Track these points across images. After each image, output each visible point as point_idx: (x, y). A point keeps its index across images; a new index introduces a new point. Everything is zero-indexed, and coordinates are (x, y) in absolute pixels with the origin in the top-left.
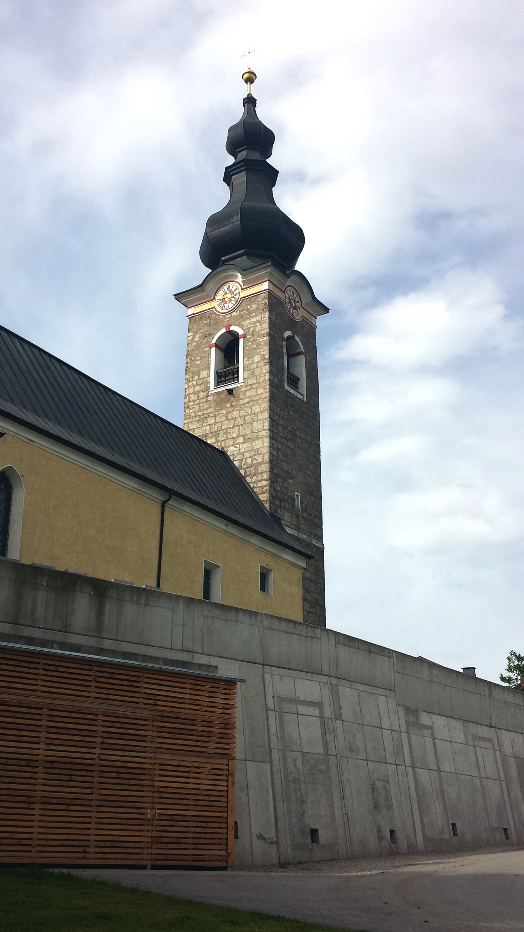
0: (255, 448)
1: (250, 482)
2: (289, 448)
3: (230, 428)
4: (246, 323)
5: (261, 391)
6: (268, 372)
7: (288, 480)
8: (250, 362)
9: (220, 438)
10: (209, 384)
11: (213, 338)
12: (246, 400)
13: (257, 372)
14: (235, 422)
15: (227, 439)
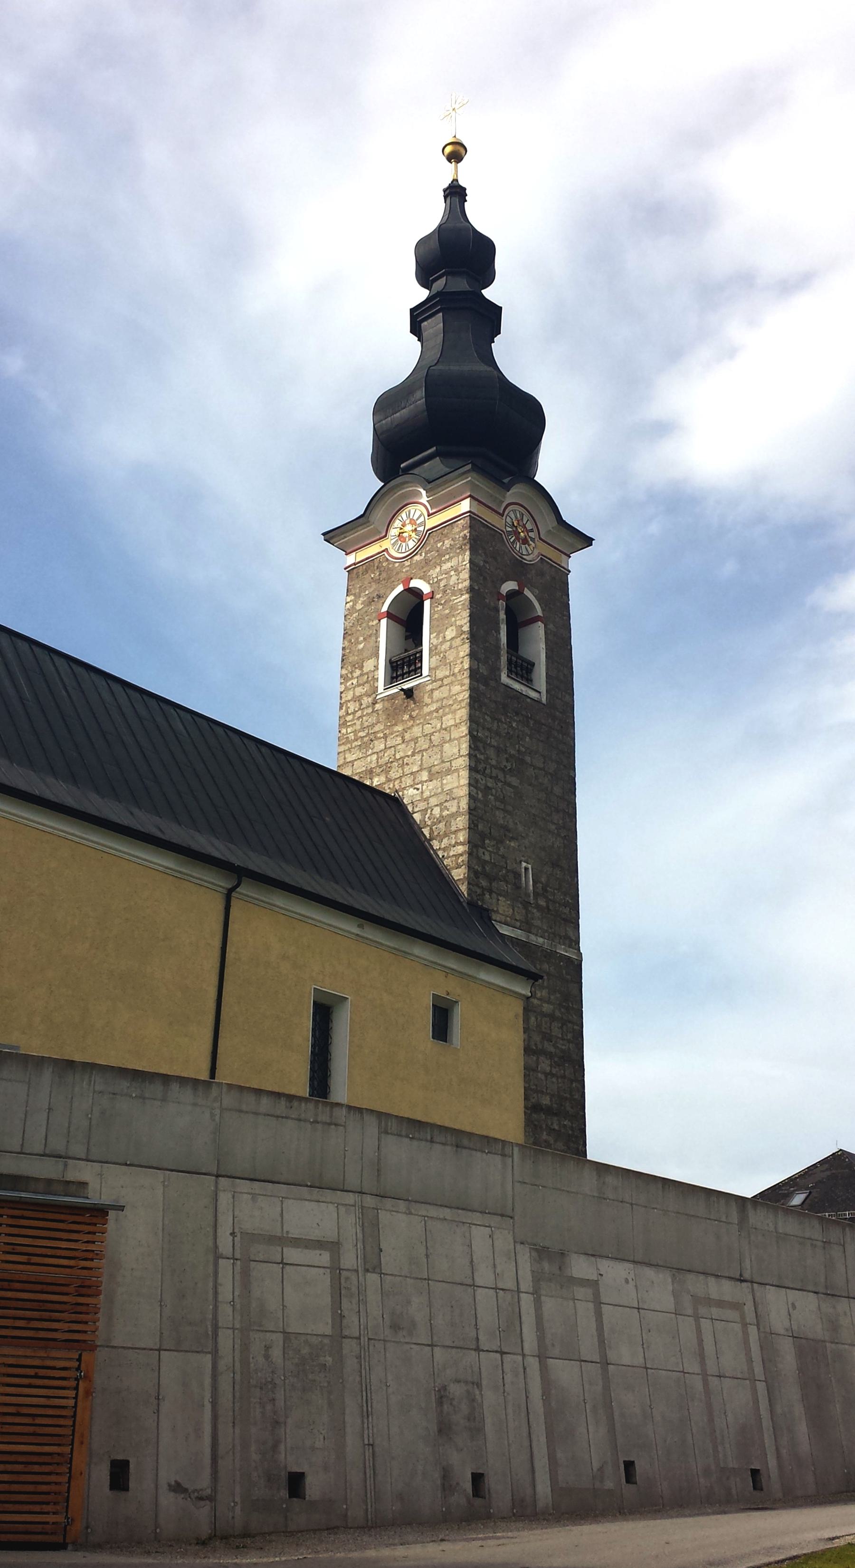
0: (446, 788)
1: (438, 848)
2: (510, 785)
3: (408, 756)
4: (434, 572)
5: (456, 688)
6: (467, 655)
7: (508, 842)
8: (441, 639)
9: (393, 774)
10: (377, 681)
11: (383, 603)
12: (433, 707)
13: (451, 656)
14: (415, 746)
15: (404, 775)
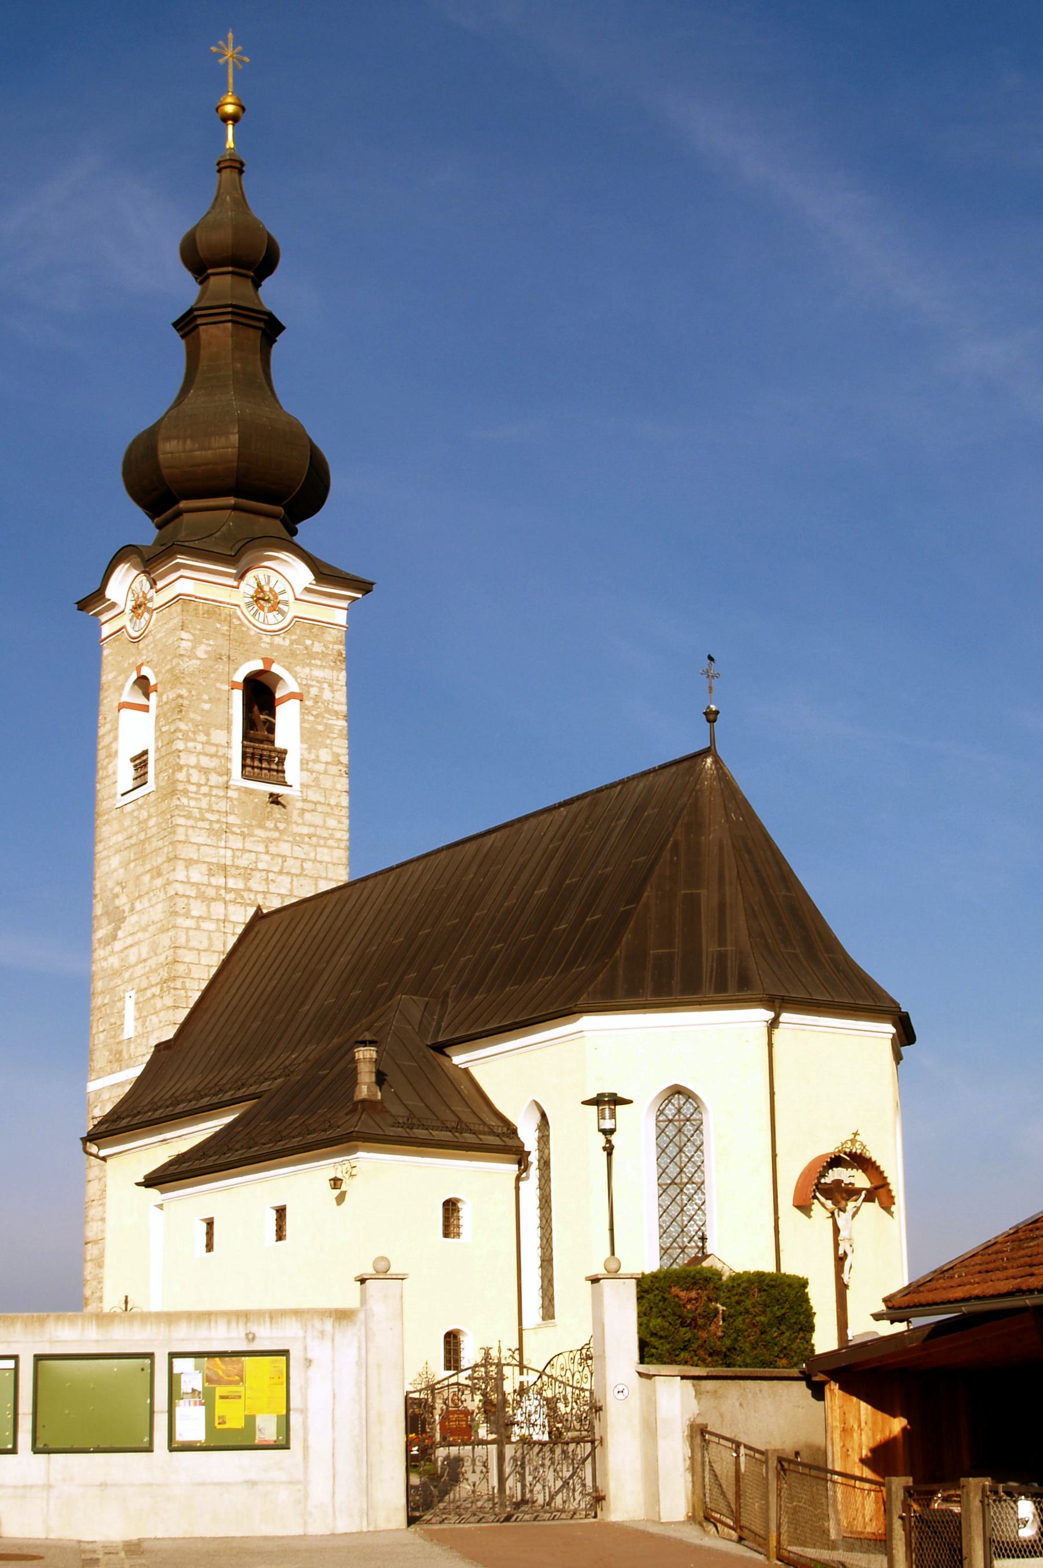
3: (275, 873)
8: (313, 757)
9: (256, 884)
12: (305, 830)
15: (268, 892)
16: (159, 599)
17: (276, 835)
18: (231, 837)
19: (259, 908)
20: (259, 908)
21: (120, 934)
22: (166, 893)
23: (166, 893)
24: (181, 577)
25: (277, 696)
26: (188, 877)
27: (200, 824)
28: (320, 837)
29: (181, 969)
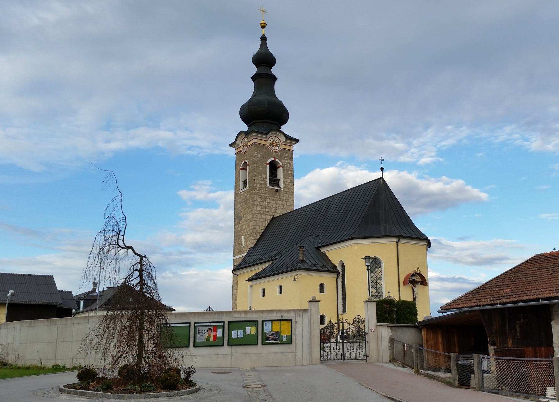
8: (286, 181)
9: (272, 211)
16: (249, 144)
17: (277, 199)
18: (267, 200)
19: (273, 216)
20: (273, 216)
21: (241, 222)
22: (251, 212)
23: (251, 212)
24: (254, 138)
25: (277, 167)
26: (257, 209)
27: (259, 196)
28: (288, 200)
29: (255, 230)
